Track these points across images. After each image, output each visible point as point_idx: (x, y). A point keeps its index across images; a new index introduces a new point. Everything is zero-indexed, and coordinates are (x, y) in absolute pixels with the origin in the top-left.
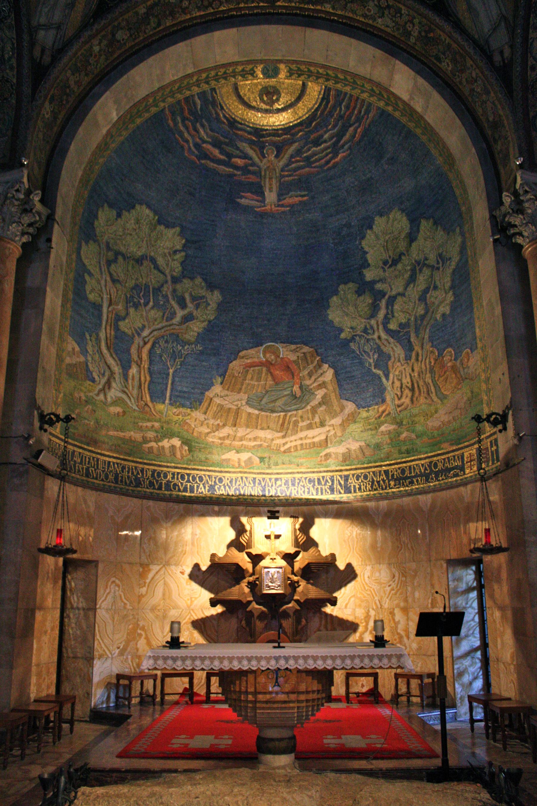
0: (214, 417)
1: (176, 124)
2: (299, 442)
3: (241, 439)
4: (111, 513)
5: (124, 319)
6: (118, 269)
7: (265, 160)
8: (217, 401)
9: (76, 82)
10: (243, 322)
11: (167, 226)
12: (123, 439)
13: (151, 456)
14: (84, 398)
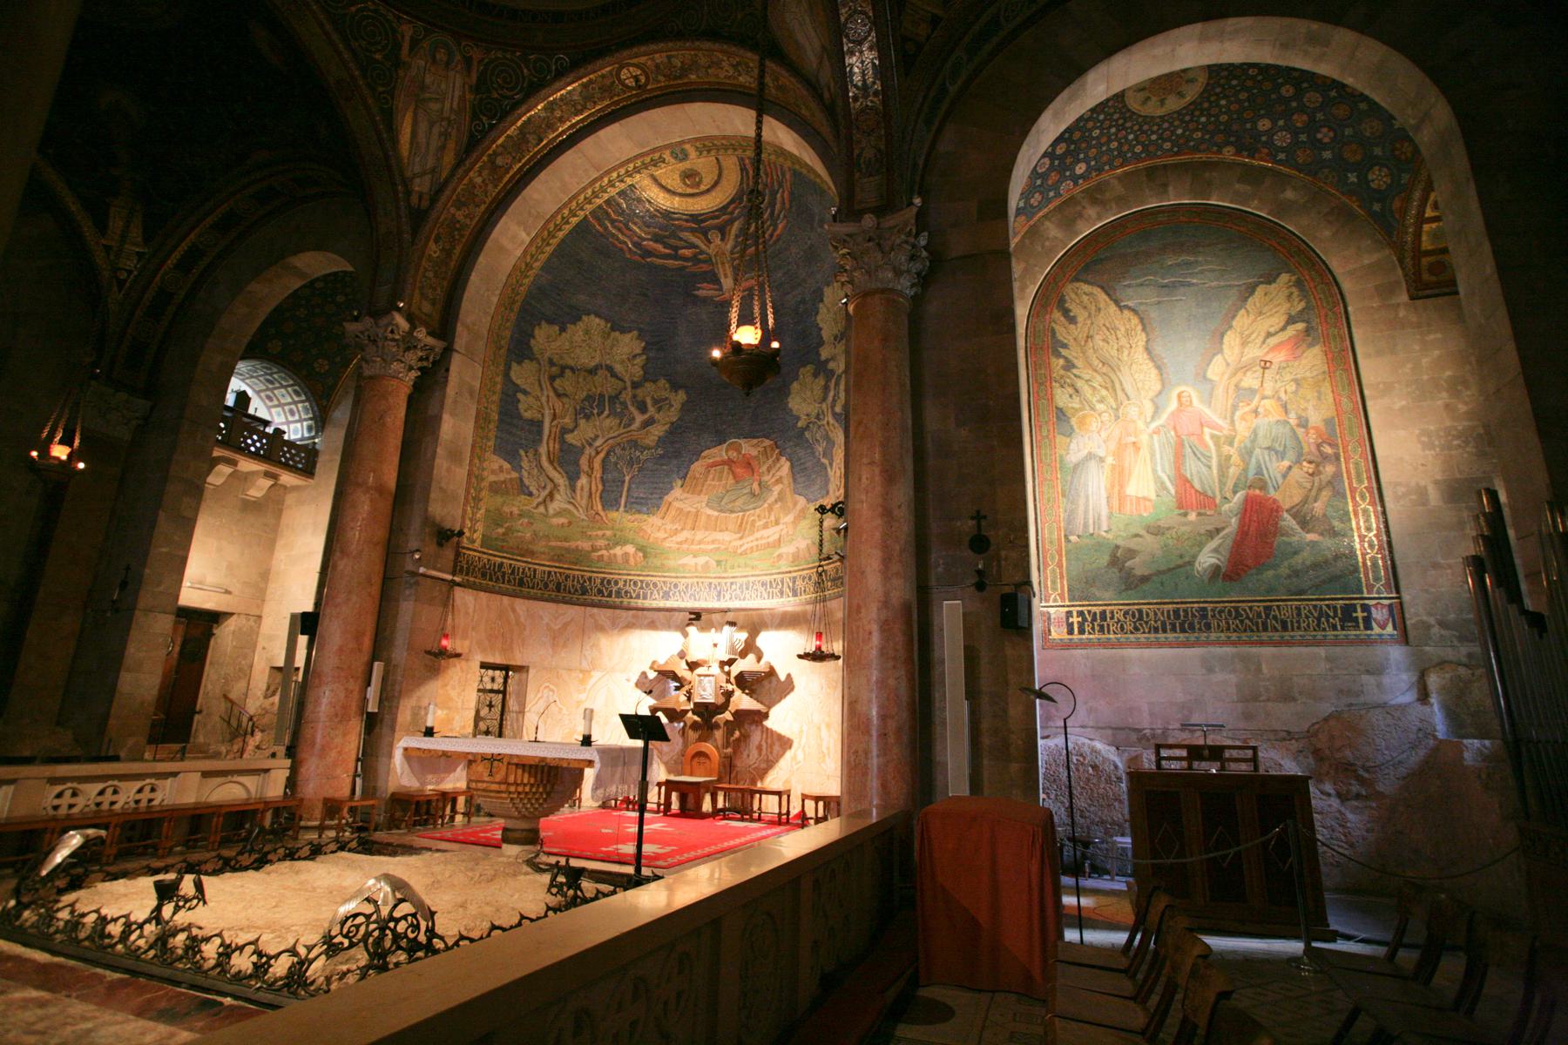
0: (673, 522)
1: (606, 228)
2: (755, 543)
3: (700, 543)
4: (546, 620)
5: (572, 431)
6: (565, 384)
7: (712, 246)
8: (677, 504)
9: (466, 217)
10: (708, 420)
11: (623, 331)
12: (568, 550)
13: (600, 564)
14: (516, 510)
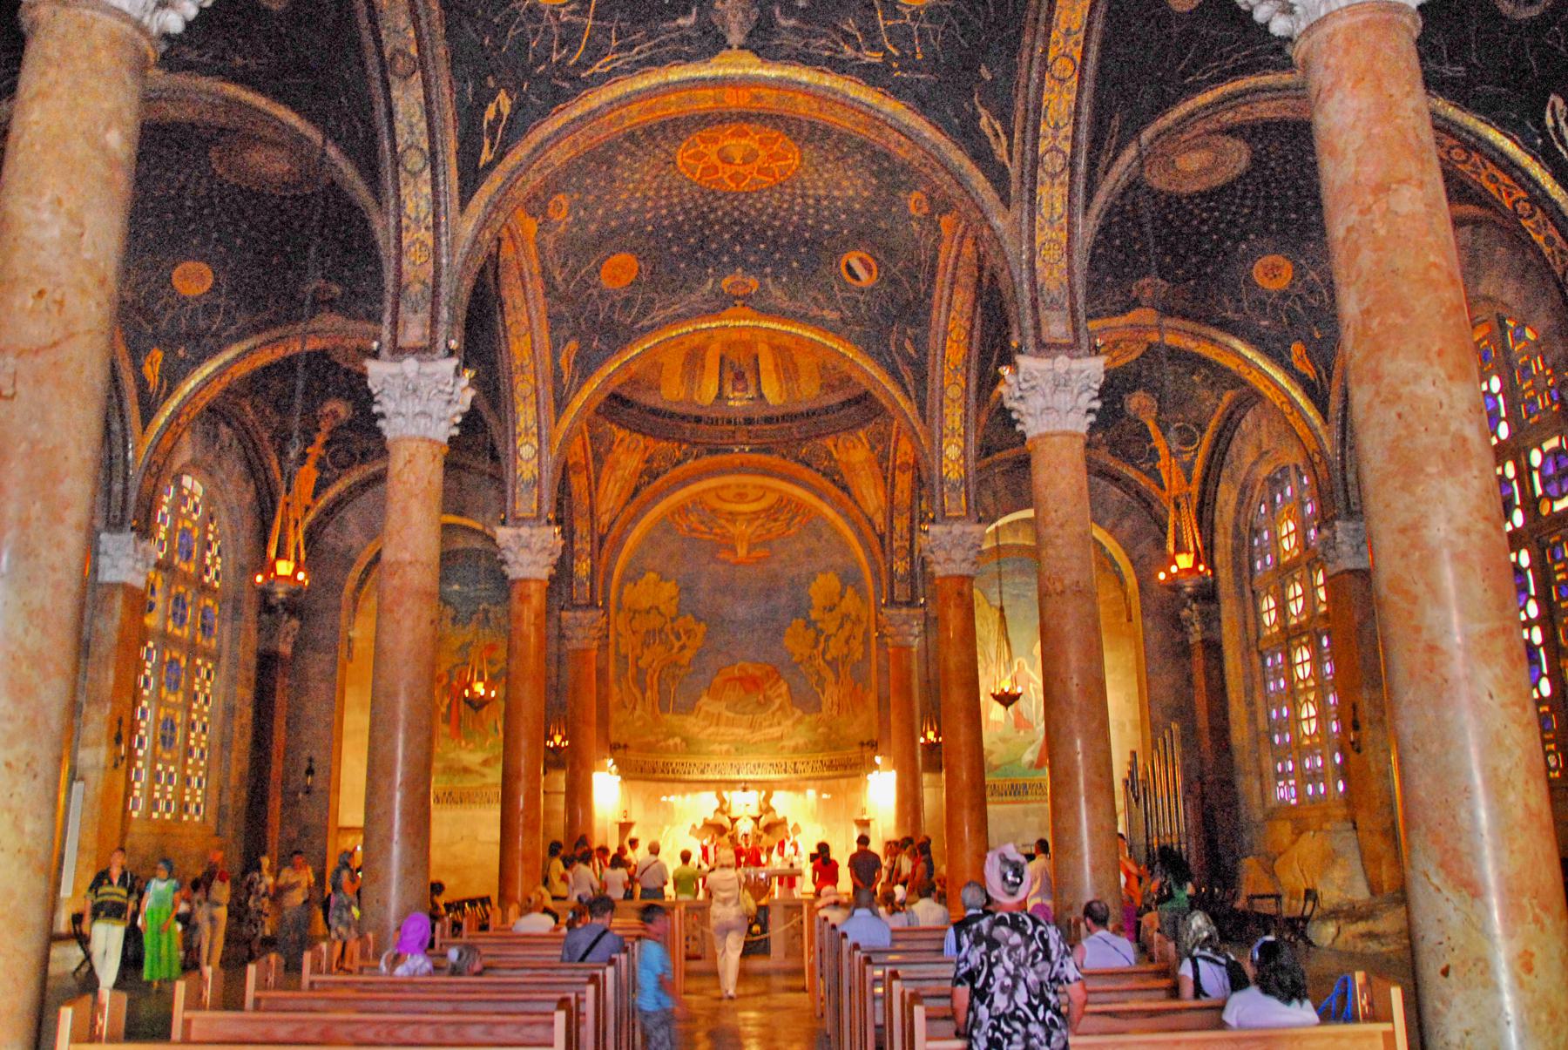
8: (705, 708)
11: (667, 580)
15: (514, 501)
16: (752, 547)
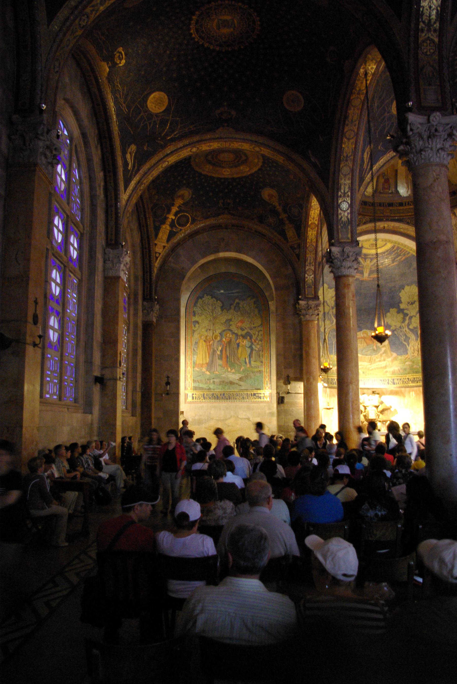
7: (366, 263)
15: (338, 233)
16: (371, 272)
